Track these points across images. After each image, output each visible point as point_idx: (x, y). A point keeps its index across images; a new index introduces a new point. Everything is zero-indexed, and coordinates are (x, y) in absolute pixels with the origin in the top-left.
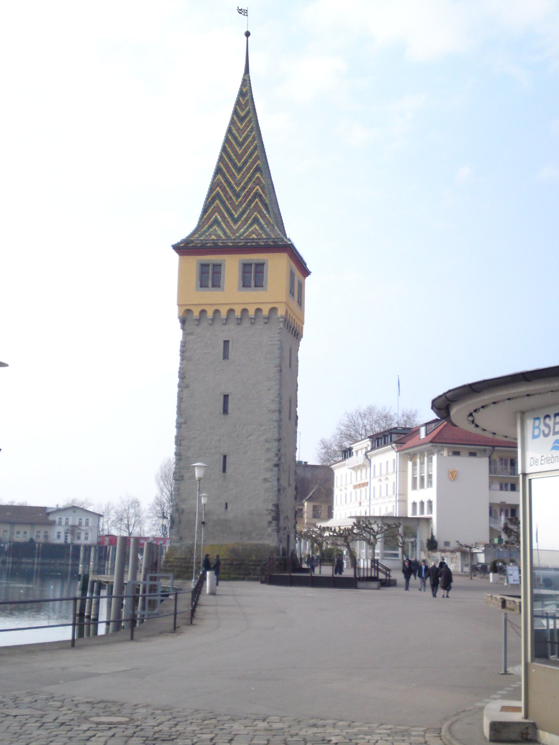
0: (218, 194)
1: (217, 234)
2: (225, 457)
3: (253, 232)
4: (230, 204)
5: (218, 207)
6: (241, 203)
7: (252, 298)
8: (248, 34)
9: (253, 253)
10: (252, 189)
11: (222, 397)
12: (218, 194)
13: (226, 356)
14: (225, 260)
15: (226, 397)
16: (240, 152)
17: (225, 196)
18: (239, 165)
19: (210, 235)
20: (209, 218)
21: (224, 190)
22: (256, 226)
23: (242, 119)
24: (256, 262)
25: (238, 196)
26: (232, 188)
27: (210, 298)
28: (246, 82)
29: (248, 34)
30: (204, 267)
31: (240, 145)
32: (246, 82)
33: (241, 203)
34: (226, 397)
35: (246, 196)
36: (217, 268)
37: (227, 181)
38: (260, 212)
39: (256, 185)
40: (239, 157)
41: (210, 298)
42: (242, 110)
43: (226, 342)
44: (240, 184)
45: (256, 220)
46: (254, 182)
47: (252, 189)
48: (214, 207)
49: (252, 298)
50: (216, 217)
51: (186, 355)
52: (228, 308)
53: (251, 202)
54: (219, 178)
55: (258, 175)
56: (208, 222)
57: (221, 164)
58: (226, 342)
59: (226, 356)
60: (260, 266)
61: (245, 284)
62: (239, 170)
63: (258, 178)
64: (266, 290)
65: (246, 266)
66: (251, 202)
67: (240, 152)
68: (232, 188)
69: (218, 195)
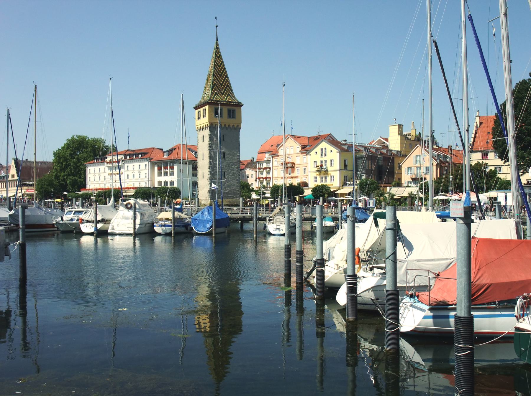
1: (218, 98)
3: (229, 99)
6: (223, 88)
8: (217, 26)
19: (216, 98)
23: (218, 57)
28: (217, 44)
31: (219, 67)
33: (223, 88)
35: (224, 85)
40: (220, 71)
45: (229, 95)
53: (226, 87)
60: (234, 111)
62: (221, 76)
65: (229, 111)
66: (226, 87)
69: (215, 84)
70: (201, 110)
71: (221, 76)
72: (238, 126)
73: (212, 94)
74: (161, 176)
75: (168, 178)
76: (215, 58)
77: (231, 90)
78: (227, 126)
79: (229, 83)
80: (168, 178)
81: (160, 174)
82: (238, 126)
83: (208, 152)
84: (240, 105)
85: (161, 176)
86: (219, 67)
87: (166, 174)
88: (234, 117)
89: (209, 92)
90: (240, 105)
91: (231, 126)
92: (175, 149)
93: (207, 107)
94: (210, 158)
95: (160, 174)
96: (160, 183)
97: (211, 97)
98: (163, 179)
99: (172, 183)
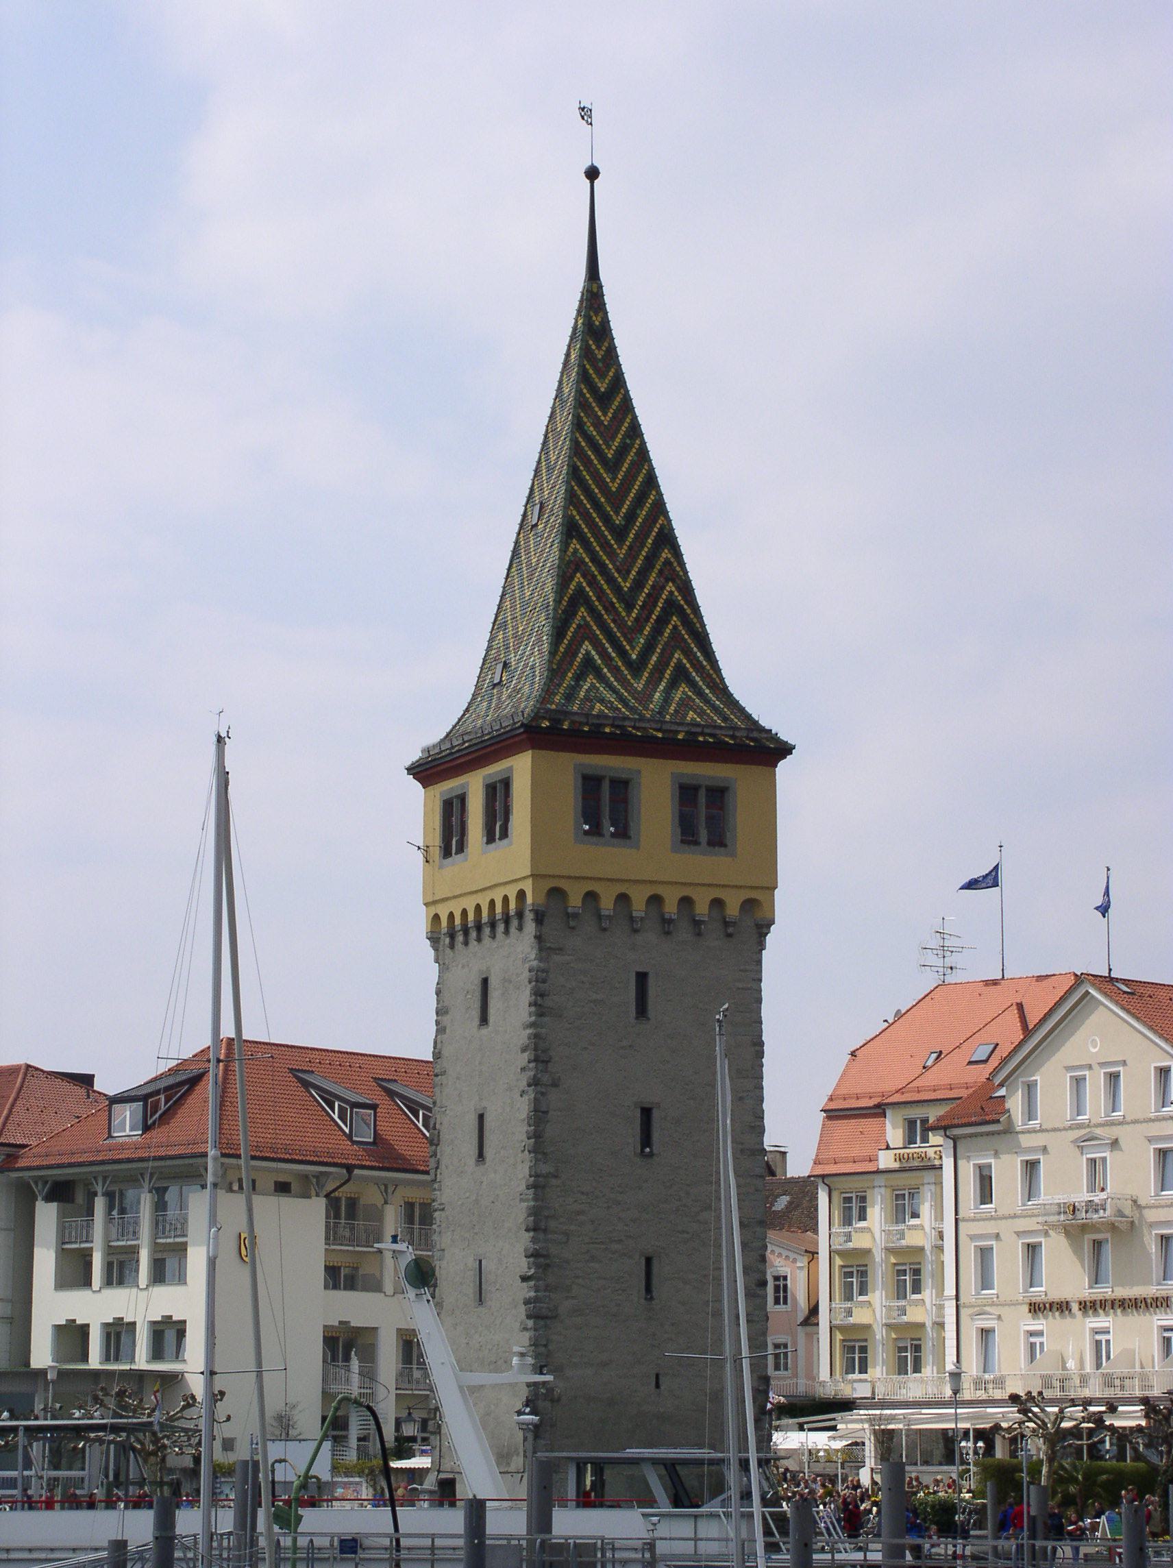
0: (580, 591)
1: (601, 699)
2: (649, 1261)
3: (685, 704)
4: (614, 621)
5: (587, 625)
6: (640, 623)
7: (700, 871)
8: (592, 174)
9: (726, 762)
10: (657, 589)
11: (638, 1113)
12: (580, 591)
13: (642, 1009)
14: (639, 772)
15: (646, 1112)
16: (614, 487)
17: (599, 599)
18: (618, 521)
20: (572, 652)
21: (592, 582)
22: (683, 690)
23: (604, 400)
24: (708, 783)
25: (629, 607)
26: (611, 580)
27: (607, 863)
28: (593, 300)
29: (592, 174)
30: (590, 784)
31: (613, 467)
32: (593, 300)
33: (640, 623)
34: (646, 1112)
36: (622, 787)
37: (595, 559)
38: (688, 653)
39: (667, 580)
41: (607, 863)
42: (602, 375)
43: (642, 978)
44: (629, 572)
45: (681, 675)
46: (661, 572)
47: (657, 589)
48: (579, 626)
49: (700, 871)
50: (588, 653)
51: (548, 1002)
52: (649, 891)
53: (662, 621)
54: (576, 550)
55: (666, 554)
56: (571, 664)
57: (575, 513)
58: (642, 978)
59: (642, 1009)
60: (719, 794)
61: (687, 834)
62: (620, 534)
63: (667, 563)
64: (733, 855)
65: (687, 793)
66: (662, 621)
67: (614, 487)
68: (611, 580)
69: (579, 598)
70: (474, 785)
71: (620, 534)
72: (750, 905)
73: (555, 672)
74: (85, 1281)
75: (141, 1304)
76: (581, 403)
77: (702, 639)
78: (671, 908)
79: (686, 589)
80: (141, 1304)
81: (75, 1272)
82: (750, 905)
83: (523, 1107)
84: (768, 751)
85: (85, 1281)
86: (613, 467)
87: (120, 1271)
88: (718, 841)
89: (533, 658)
90: (768, 751)
91: (702, 908)
92: (195, 1081)
93: (521, 768)
94: (539, 1143)
95: (75, 1272)
96: (72, 1336)
97: (547, 693)
98: (96, 1307)
99: (167, 1334)
